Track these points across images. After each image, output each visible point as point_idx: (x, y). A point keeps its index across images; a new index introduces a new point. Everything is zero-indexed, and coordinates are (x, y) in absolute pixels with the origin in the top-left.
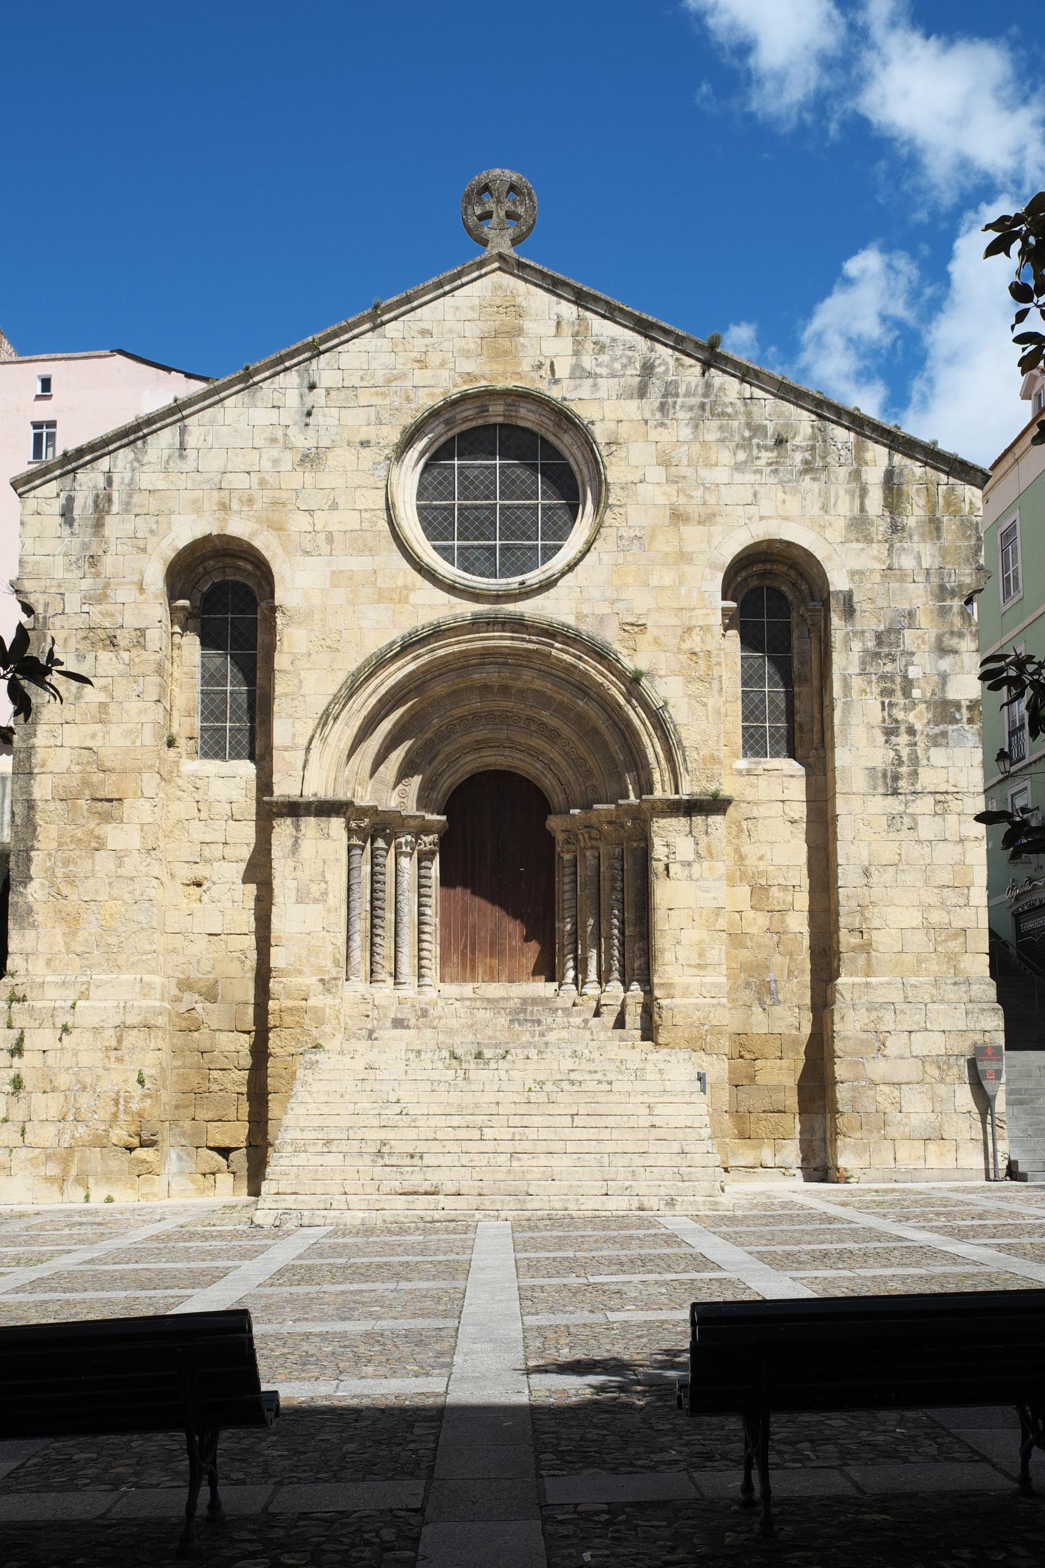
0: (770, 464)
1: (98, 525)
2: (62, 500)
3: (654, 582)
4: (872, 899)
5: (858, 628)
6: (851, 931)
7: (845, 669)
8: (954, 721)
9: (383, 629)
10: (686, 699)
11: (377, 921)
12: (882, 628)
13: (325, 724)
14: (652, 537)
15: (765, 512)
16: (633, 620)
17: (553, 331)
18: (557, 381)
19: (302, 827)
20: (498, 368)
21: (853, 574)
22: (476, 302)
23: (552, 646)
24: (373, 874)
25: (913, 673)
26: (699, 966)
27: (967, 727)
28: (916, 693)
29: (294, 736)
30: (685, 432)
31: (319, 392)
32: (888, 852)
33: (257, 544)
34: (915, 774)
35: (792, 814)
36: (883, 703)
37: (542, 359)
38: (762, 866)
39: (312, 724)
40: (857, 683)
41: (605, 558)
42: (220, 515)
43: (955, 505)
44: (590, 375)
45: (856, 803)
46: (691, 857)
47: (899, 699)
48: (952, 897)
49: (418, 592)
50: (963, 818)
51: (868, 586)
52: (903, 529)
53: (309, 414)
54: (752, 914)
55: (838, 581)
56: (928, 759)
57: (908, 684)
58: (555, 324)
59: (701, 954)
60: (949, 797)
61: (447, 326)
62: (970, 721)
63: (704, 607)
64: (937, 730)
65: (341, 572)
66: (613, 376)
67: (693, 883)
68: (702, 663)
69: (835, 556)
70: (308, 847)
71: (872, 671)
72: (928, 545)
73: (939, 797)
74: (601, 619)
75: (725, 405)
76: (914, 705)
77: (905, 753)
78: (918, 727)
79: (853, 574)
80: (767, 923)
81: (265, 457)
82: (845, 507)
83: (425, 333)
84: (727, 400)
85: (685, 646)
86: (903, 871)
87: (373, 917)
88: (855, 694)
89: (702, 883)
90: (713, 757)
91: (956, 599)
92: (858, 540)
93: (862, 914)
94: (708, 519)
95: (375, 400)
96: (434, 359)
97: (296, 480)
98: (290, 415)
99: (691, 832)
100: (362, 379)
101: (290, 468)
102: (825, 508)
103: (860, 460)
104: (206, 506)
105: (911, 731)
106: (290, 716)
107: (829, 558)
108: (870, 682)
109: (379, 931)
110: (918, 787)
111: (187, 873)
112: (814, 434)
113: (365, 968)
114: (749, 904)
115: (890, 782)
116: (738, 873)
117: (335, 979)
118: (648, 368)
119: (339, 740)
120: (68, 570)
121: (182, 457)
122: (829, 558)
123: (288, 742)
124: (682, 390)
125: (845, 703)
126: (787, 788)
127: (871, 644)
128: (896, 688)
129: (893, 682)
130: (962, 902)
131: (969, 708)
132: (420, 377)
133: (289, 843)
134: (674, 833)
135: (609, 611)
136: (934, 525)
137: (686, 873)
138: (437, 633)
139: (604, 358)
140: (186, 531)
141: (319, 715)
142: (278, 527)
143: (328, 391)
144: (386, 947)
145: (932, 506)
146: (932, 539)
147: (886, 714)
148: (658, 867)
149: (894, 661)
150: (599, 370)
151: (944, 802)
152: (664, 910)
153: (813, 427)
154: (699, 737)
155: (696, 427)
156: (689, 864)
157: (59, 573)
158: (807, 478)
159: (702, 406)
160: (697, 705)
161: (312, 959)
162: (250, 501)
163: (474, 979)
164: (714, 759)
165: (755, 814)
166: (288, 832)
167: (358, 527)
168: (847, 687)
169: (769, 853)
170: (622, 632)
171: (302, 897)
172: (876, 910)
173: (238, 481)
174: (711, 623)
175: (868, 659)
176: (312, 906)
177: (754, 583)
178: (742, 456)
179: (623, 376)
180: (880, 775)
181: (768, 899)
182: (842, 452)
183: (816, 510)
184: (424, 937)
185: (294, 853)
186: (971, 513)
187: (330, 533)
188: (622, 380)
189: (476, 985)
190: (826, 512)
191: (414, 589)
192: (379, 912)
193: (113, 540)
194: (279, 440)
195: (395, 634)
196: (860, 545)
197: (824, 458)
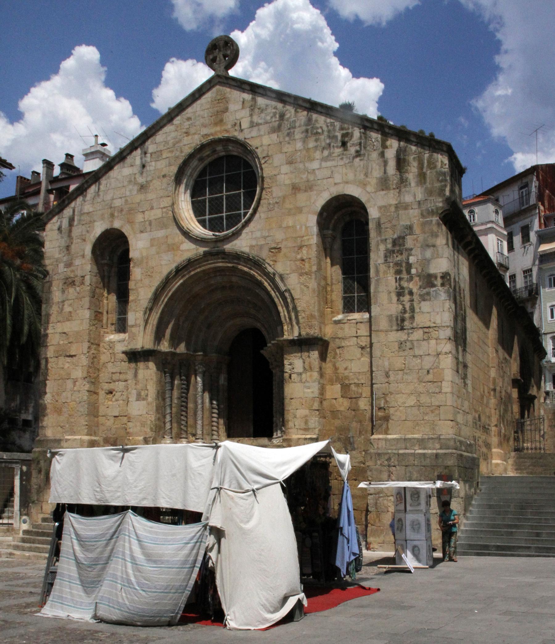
0: (339, 156)
1: (70, 231)
2: (59, 223)
3: (284, 225)
4: (390, 390)
5: (383, 238)
6: (380, 409)
7: (376, 261)
8: (433, 286)
9: (167, 264)
10: (299, 285)
12: (395, 236)
14: (284, 201)
15: (336, 181)
17: (241, 107)
18: (242, 130)
20: (218, 129)
21: (380, 208)
22: (209, 100)
25: (412, 259)
27: (440, 288)
28: (413, 271)
30: (299, 145)
31: (148, 155)
32: (398, 363)
33: (124, 231)
34: (412, 318)
36: (396, 278)
37: (236, 121)
38: (346, 373)
40: (382, 268)
41: (263, 215)
42: (110, 219)
43: (433, 163)
44: (258, 124)
45: (382, 335)
46: (301, 370)
47: (405, 276)
48: (432, 388)
50: (439, 341)
51: (388, 214)
52: (406, 181)
53: (144, 166)
54: (341, 400)
55: (373, 213)
56: (420, 309)
57: (409, 266)
58: (241, 103)
59: (306, 422)
60: (431, 330)
61: (198, 113)
62: (443, 285)
63: (308, 235)
64: (425, 291)
65: (154, 239)
66: (266, 123)
68: (307, 265)
69: (371, 199)
71: (391, 261)
72: (420, 188)
73: (426, 330)
74: (261, 247)
75: (317, 128)
76: (411, 279)
77: (407, 306)
78: (415, 290)
79: (380, 208)
80: (349, 405)
81: (128, 189)
82: (377, 173)
83: (189, 119)
84: (318, 125)
85: (299, 257)
86: (406, 374)
88: (381, 275)
89: (307, 384)
90: (311, 315)
91: (435, 216)
92: (383, 190)
93: (385, 399)
94: (309, 187)
95: (169, 155)
96: (192, 131)
97: (139, 197)
98: (136, 169)
100: (164, 146)
101: (135, 192)
102: (366, 175)
103: (384, 146)
104: (106, 216)
105: (411, 293)
106: (134, 311)
107: (368, 201)
108: (389, 267)
110: (415, 325)
111: (106, 387)
112: (361, 136)
113: (175, 430)
114: (340, 394)
115: (400, 323)
116: (335, 378)
118: (282, 116)
120: (60, 254)
121: (99, 195)
122: (368, 201)
124: (297, 124)
125: (376, 280)
126: (359, 329)
127: (389, 246)
128: (402, 269)
129: (401, 266)
130: (437, 390)
131: (442, 277)
132: (186, 140)
136: (422, 177)
137: (299, 379)
138: (190, 264)
139: (263, 115)
140: (99, 229)
142: (131, 222)
143: (151, 154)
145: (421, 166)
146: (421, 184)
147: (398, 284)
148: (286, 375)
149: (402, 254)
150: (260, 121)
151: (428, 333)
152: (289, 399)
153: (360, 132)
155: (304, 142)
156: (300, 374)
157: (57, 256)
158: (357, 160)
159: (307, 131)
160: (305, 289)
162: (122, 210)
164: (312, 316)
165: (343, 344)
167: (160, 216)
168: (377, 272)
169: (350, 366)
170: (270, 253)
171: (139, 397)
172: (392, 396)
173: (118, 203)
175: (388, 254)
176: (142, 402)
177: (347, 219)
178: (326, 153)
179: (271, 122)
180: (394, 319)
181: (349, 390)
182: (375, 143)
183: (362, 176)
186: (442, 167)
187: (150, 221)
188: (271, 124)
190: (367, 176)
191: (182, 243)
193: (75, 238)
194: (132, 181)
195: (173, 266)
196: (384, 192)
197: (365, 148)
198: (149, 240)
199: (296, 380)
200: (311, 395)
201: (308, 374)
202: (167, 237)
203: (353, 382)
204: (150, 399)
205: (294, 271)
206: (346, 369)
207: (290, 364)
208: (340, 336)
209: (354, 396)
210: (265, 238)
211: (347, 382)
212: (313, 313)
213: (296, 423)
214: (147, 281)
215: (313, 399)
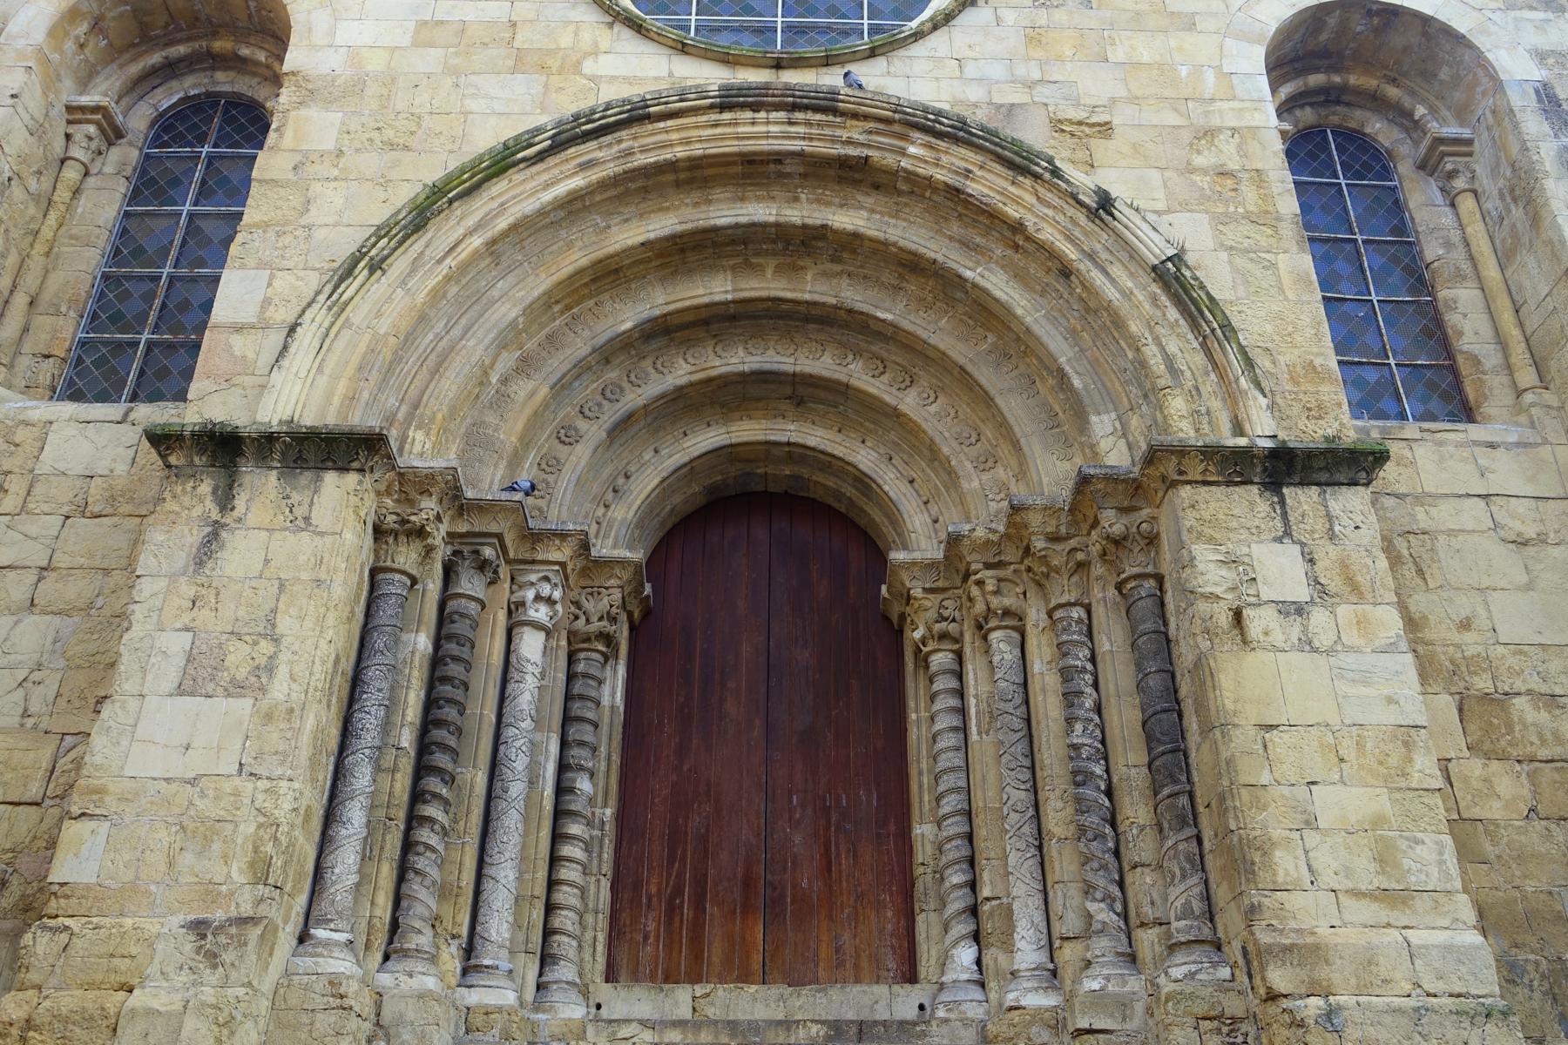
3: (1118, 54)
10: (1224, 256)
11: (433, 784)
13: (348, 272)
16: (1080, 115)
19: (240, 503)
21: (1541, 56)
23: (903, 152)
24: (436, 661)
26: (1383, 895)
29: (267, 302)
35: (1517, 525)
38: (1472, 643)
39: (314, 280)
41: (1009, 16)
46: (1302, 593)
49: (602, 58)
54: (1474, 768)
59: (1385, 858)
67: (1321, 660)
70: (242, 553)
79: (1541, 56)
87: (422, 769)
89: (1349, 660)
99: (1288, 533)
109: (432, 810)
117: (243, 921)
119: (379, 315)
123: (248, 315)
133: (193, 536)
134: (1244, 535)
135: (1025, 99)
137: (1296, 632)
138: (637, 115)
141: (336, 265)
144: (447, 856)
152: (1252, 732)
154: (1269, 328)
156: (1300, 610)
161: (187, 859)
163: (695, 978)
166: (197, 511)
174: (1256, 124)
176: (221, 703)
184: (567, 850)
185: (200, 564)
189: (699, 990)
191: (595, 52)
192: (441, 760)
198: (411, 26)
199: (1278, 638)
200: (1390, 717)
201: (1344, 611)
202: (514, 25)
203: (1519, 685)
204: (280, 688)
205: (1185, 207)
206: (1465, 625)
207: (1231, 562)
208: (1403, 490)
209: (1543, 753)
210: (1030, 85)
211: (1483, 683)
212: (1318, 361)
213: (1322, 859)
214: (371, 162)
215: (1406, 734)
